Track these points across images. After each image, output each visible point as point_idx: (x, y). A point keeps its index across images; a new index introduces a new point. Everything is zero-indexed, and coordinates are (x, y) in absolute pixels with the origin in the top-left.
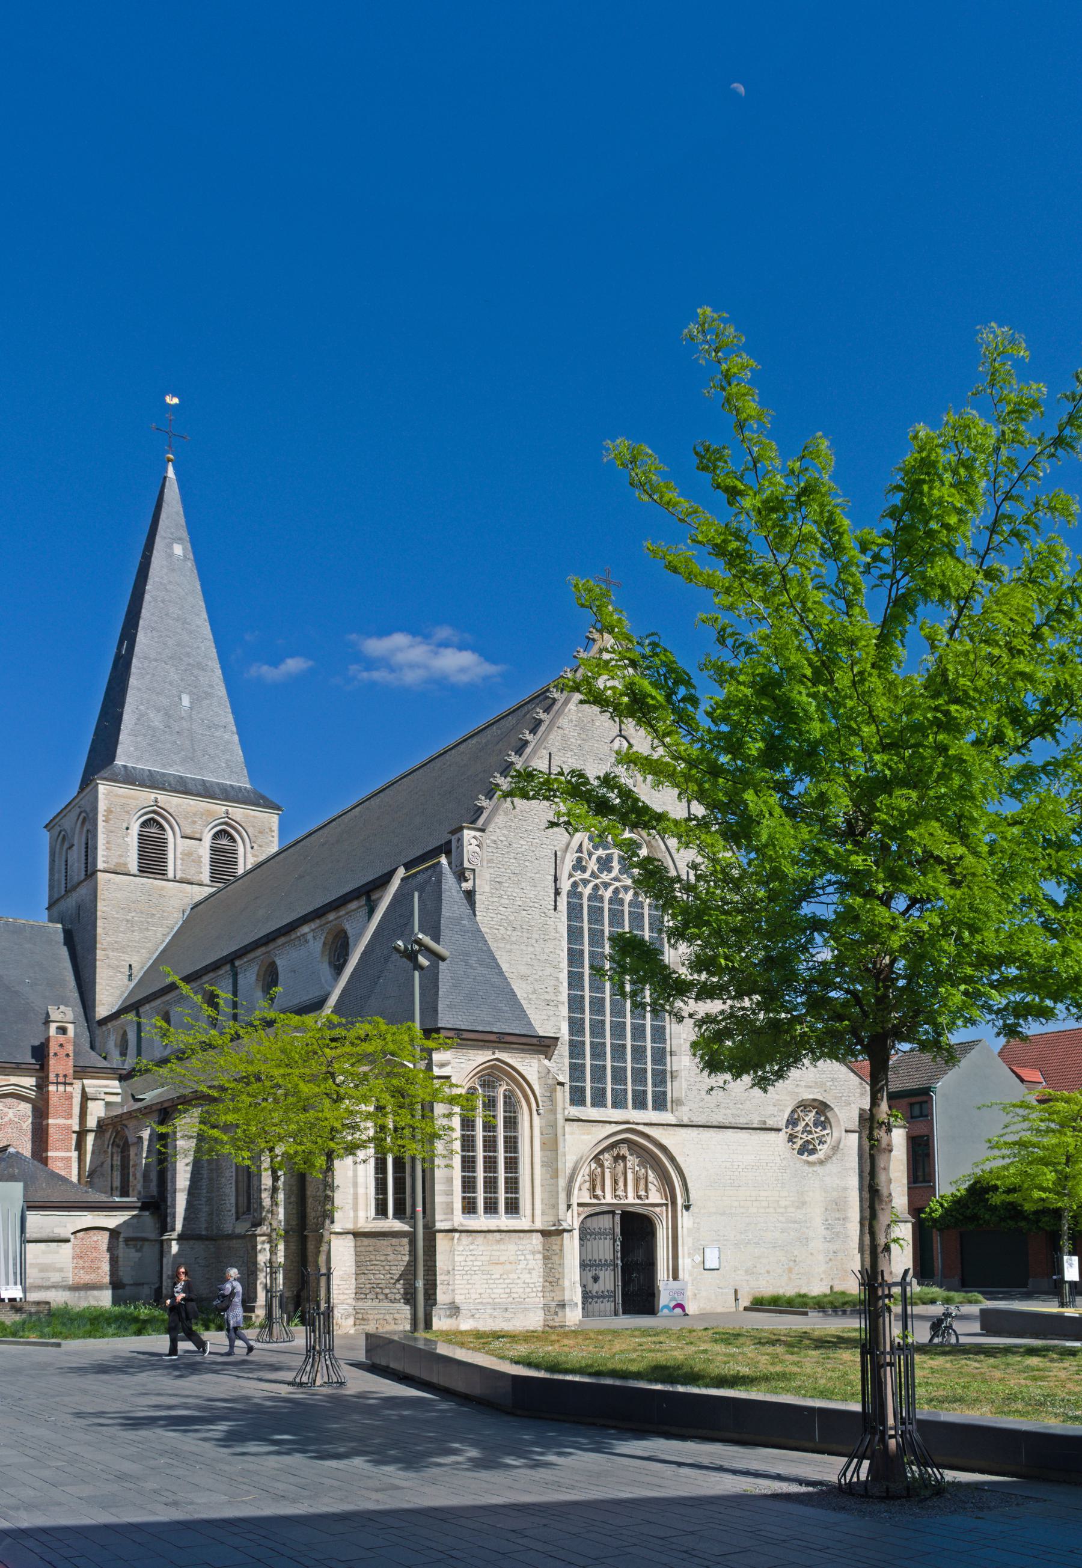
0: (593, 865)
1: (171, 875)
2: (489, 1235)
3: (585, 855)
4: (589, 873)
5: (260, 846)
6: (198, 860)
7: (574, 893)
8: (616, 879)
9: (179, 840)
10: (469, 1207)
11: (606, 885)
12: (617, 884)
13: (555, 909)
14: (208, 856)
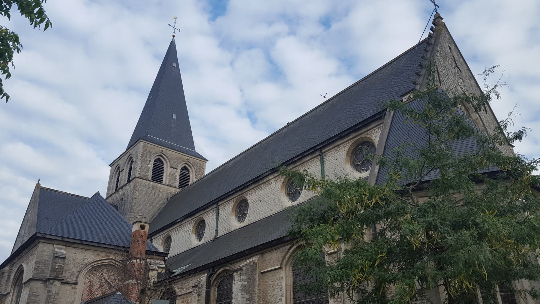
1: (164, 182)
5: (198, 174)
6: (175, 178)
9: (169, 168)
14: (179, 176)
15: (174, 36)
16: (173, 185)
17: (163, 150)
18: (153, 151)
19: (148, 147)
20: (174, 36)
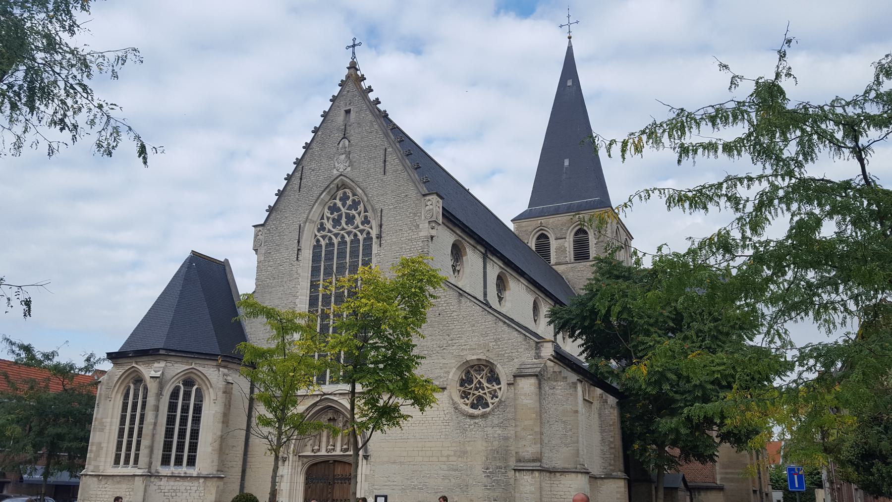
0: (329, 225)
2: (115, 479)
3: (325, 221)
4: (327, 229)
7: (317, 246)
8: (343, 229)
10: (117, 462)
11: (336, 235)
12: (342, 232)
13: (297, 260)
15: (570, 38)
16: (563, 261)
17: (542, 221)
18: (530, 229)
19: (523, 227)
20: (570, 38)
